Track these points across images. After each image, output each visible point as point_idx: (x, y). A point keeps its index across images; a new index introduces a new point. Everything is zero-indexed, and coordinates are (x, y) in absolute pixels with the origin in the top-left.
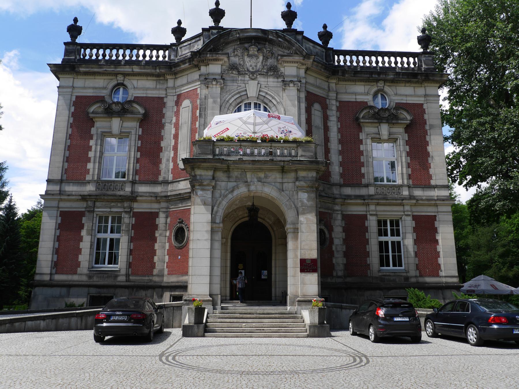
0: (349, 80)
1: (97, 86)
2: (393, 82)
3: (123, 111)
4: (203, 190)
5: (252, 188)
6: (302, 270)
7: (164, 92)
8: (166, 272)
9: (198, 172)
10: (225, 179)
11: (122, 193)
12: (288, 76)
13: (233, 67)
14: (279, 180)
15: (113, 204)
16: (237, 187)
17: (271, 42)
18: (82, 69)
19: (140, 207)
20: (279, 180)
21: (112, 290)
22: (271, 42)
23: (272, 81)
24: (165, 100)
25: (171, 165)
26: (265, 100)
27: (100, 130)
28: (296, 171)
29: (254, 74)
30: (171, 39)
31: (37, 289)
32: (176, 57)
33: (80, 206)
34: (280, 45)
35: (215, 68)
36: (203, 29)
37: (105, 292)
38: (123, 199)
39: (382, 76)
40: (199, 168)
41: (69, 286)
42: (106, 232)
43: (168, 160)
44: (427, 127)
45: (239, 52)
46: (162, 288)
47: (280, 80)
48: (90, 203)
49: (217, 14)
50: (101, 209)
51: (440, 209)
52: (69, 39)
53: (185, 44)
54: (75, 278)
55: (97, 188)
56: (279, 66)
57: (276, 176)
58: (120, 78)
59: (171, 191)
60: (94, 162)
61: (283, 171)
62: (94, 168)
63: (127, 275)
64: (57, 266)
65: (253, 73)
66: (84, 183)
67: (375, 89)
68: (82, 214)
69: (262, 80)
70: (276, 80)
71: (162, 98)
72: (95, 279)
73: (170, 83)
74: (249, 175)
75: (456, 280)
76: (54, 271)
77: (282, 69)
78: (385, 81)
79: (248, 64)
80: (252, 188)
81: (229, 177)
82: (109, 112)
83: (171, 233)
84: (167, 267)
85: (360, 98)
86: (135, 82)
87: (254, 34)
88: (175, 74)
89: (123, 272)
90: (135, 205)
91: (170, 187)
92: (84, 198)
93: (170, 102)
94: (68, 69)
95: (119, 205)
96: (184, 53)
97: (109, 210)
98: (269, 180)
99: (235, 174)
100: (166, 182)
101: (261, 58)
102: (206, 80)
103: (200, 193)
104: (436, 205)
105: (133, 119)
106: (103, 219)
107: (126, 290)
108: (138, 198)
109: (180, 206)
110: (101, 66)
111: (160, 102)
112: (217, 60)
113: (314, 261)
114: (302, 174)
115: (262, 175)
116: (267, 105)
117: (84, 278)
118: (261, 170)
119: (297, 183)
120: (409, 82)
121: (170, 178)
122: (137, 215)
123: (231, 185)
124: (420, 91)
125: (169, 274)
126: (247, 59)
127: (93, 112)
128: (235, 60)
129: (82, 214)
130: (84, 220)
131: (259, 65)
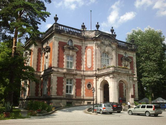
0: (120, 49)
1: (64, 39)
2: (128, 51)
3: (72, 48)
4: (115, 78)
5: (123, 79)
6: (131, 97)
7: (82, 45)
8: (85, 95)
9: (114, 74)
10: (118, 76)
11: (73, 73)
12: (114, 48)
13: (102, 43)
14: (127, 77)
15: (71, 76)
16: (120, 78)
17: (110, 38)
18: (62, 34)
19: (78, 77)
20: (127, 77)
21: (72, 101)
22: (110, 38)
23: (110, 48)
24: (82, 47)
25: (85, 66)
26: (108, 53)
27: (66, 53)
28: (130, 76)
29: (107, 46)
30: (80, 28)
31: (53, 100)
32: (84, 34)
33: (62, 76)
34: (112, 39)
35: (99, 42)
36: (95, 30)
37: (70, 101)
38: (74, 75)
39: (127, 49)
40: (114, 73)
41: (61, 99)
42: (68, 83)
43: (84, 65)
44: (133, 63)
45: (104, 39)
46: (84, 100)
47: (112, 48)
48: (65, 75)
49: (98, 26)
50: (68, 77)
51: (136, 83)
52: (55, 22)
53: (87, 32)
54: (62, 97)
55: (67, 71)
56: (111, 44)
57: (126, 76)
58: (71, 38)
59: (85, 74)
60: (66, 63)
61: (128, 76)
62: (66, 65)
63: (76, 96)
64: (58, 93)
65: (107, 45)
66: (63, 69)
67: (124, 52)
68: (63, 78)
69: (108, 47)
70: (111, 48)
71: (81, 46)
72: (68, 97)
73: (83, 42)
74: (122, 76)
75: (138, 99)
76: (56, 95)
77: (112, 45)
78: (127, 50)
79: (105, 43)
80: (123, 79)
81: (119, 76)
82: (69, 48)
83: (86, 85)
84: (85, 94)
85: (122, 54)
86: (74, 40)
87: (107, 35)
88: (85, 40)
89: (74, 95)
90: (76, 77)
91: (85, 72)
92: (64, 74)
93: (84, 48)
94: (58, 33)
95: (73, 76)
96: (87, 34)
97: (70, 77)
98: (125, 77)
99: (120, 75)
100: (84, 71)
101: (108, 41)
102: (98, 46)
103: (115, 79)
104: (135, 82)
105: (75, 51)
106: (67, 80)
107: (75, 100)
108: (78, 75)
109: (89, 78)
110: (65, 33)
111: (80, 48)
112: (100, 40)
113: (133, 95)
114: (131, 76)
115: (124, 76)
116: (108, 54)
117: (65, 97)
118: (124, 75)
119: (130, 79)
120: (131, 51)
121: (85, 70)
122: (77, 79)
123: (119, 78)
124: (132, 54)
125: (86, 96)
126: (105, 41)
127: (65, 48)
128: (103, 41)
129: (63, 78)
130: (64, 80)
131: (108, 44)
